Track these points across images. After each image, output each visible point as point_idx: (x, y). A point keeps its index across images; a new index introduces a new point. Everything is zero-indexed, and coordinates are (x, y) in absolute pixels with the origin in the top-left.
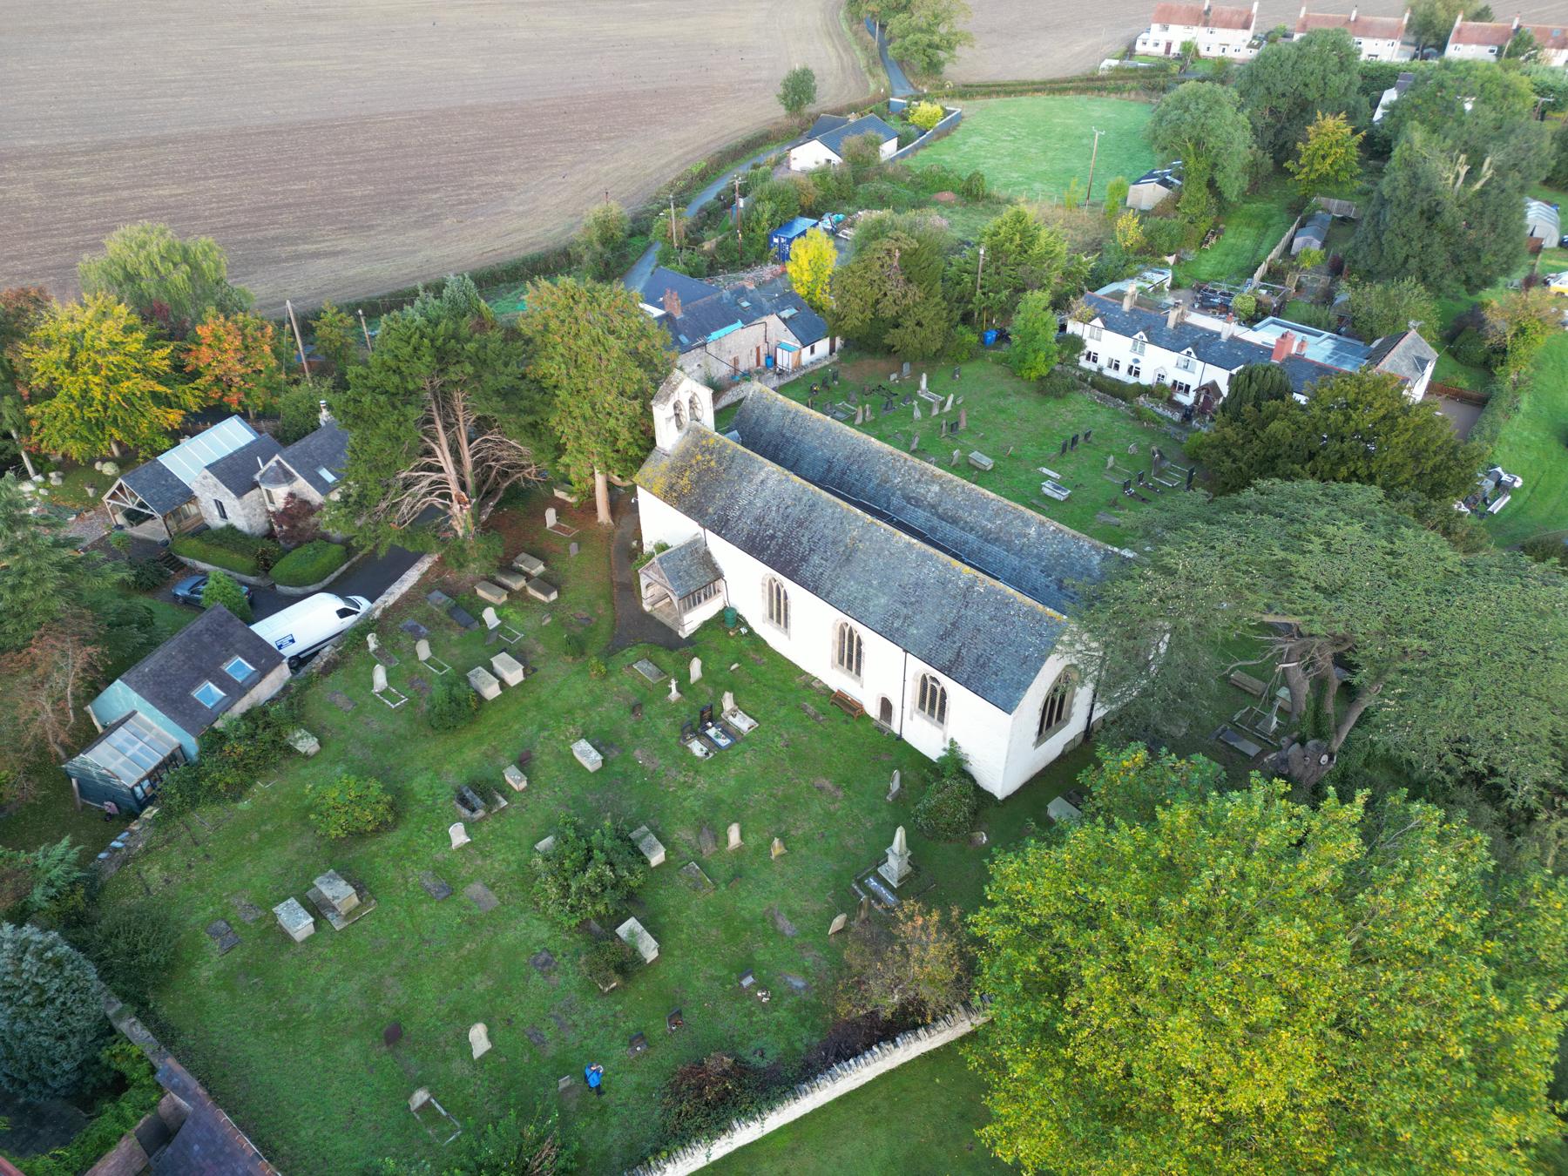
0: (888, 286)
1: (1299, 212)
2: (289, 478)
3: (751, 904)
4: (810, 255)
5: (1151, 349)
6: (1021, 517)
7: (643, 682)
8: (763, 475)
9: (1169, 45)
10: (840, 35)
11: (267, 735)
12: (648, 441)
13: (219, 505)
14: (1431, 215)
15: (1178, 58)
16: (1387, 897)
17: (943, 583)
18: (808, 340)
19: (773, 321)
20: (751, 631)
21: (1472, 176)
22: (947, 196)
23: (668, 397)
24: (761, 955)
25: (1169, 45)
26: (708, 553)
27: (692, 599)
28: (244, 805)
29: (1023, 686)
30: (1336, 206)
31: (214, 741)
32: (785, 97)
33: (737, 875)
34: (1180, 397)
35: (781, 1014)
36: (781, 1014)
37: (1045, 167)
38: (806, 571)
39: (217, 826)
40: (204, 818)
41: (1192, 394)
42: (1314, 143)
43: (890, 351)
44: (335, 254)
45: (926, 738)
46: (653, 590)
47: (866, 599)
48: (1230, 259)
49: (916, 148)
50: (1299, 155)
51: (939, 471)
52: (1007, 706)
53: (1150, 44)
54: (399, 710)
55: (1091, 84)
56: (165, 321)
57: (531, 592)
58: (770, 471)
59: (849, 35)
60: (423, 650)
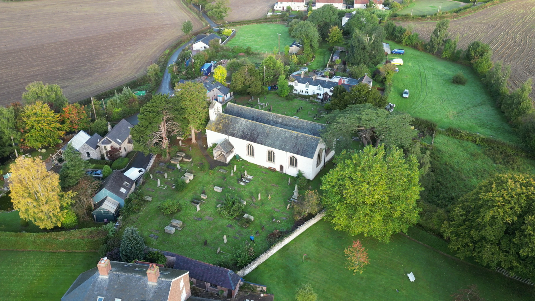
0: (246, 77)
1: (331, 50)
2: (110, 142)
3: (268, 208)
4: (221, 72)
5: (310, 86)
6: (302, 121)
7: (223, 173)
8: (241, 121)
9: (283, 8)
10: (185, 9)
11: (139, 198)
12: (207, 119)
13: (88, 154)
14: (364, 49)
15: (286, 11)
16: (391, 157)
17: (291, 136)
18: (225, 94)
19: (215, 89)
20: (243, 160)
21: (370, 40)
22: (242, 54)
23: (213, 107)
24: (274, 216)
25: (283, 8)
26: (230, 142)
27: (228, 153)
28: (141, 213)
29: (314, 153)
30: (339, 48)
31: (128, 201)
32: (184, 29)
33: (263, 204)
34: (319, 97)
35: (283, 223)
36: (283, 223)
37: (263, 44)
38: (257, 140)
39: (137, 218)
40: (133, 217)
41: (322, 96)
42: (332, 33)
44: (66, 87)
45: (292, 172)
46: (216, 154)
47: (274, 143)
48: (319, 64)
49: (227, 42)
50: (328, 37)
51: (280, 115)
52: (312, 157)
53: (278, 7)
54: (167, 189)
55: (266, 20)
56: (56, 107)
57: (185, 160)
58: (242, 120)
59: (188, 9)
60: (166, 176)
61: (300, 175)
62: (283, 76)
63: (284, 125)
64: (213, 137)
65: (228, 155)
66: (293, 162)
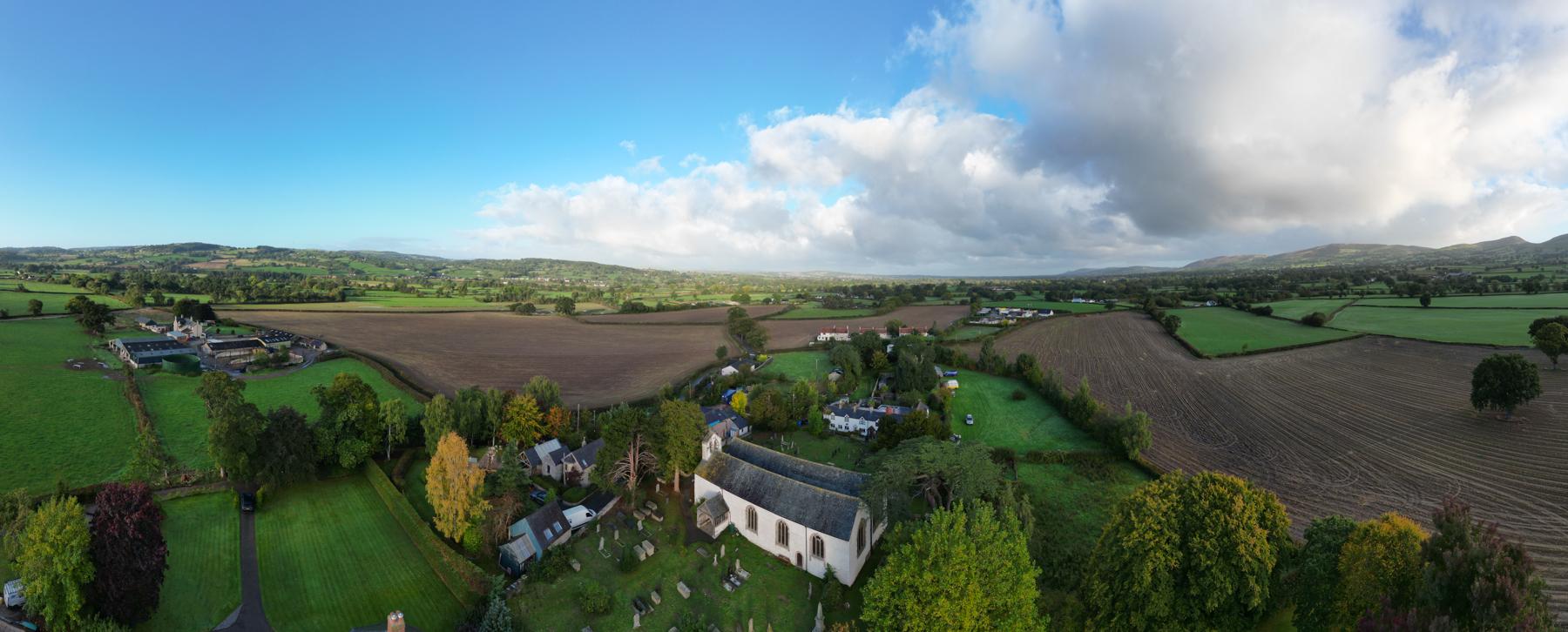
1: (877, 377)
12: (699, 458)
43: (770, 429)
46: (701, 518)
55: (808, 349)
58: (746, 465)
61: (830, 574)
62: (816, 406)
63: (807, 477)
64: (703, 487)
65: (717, 523)
66: (818, 549)
